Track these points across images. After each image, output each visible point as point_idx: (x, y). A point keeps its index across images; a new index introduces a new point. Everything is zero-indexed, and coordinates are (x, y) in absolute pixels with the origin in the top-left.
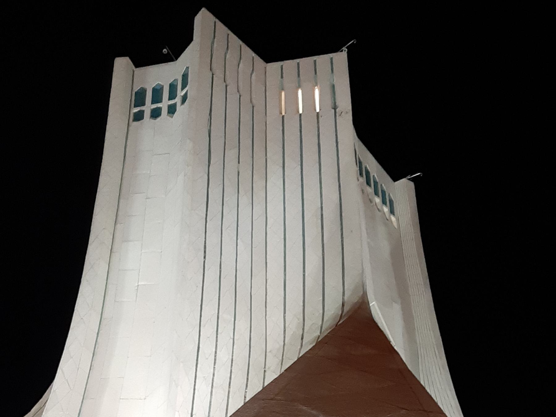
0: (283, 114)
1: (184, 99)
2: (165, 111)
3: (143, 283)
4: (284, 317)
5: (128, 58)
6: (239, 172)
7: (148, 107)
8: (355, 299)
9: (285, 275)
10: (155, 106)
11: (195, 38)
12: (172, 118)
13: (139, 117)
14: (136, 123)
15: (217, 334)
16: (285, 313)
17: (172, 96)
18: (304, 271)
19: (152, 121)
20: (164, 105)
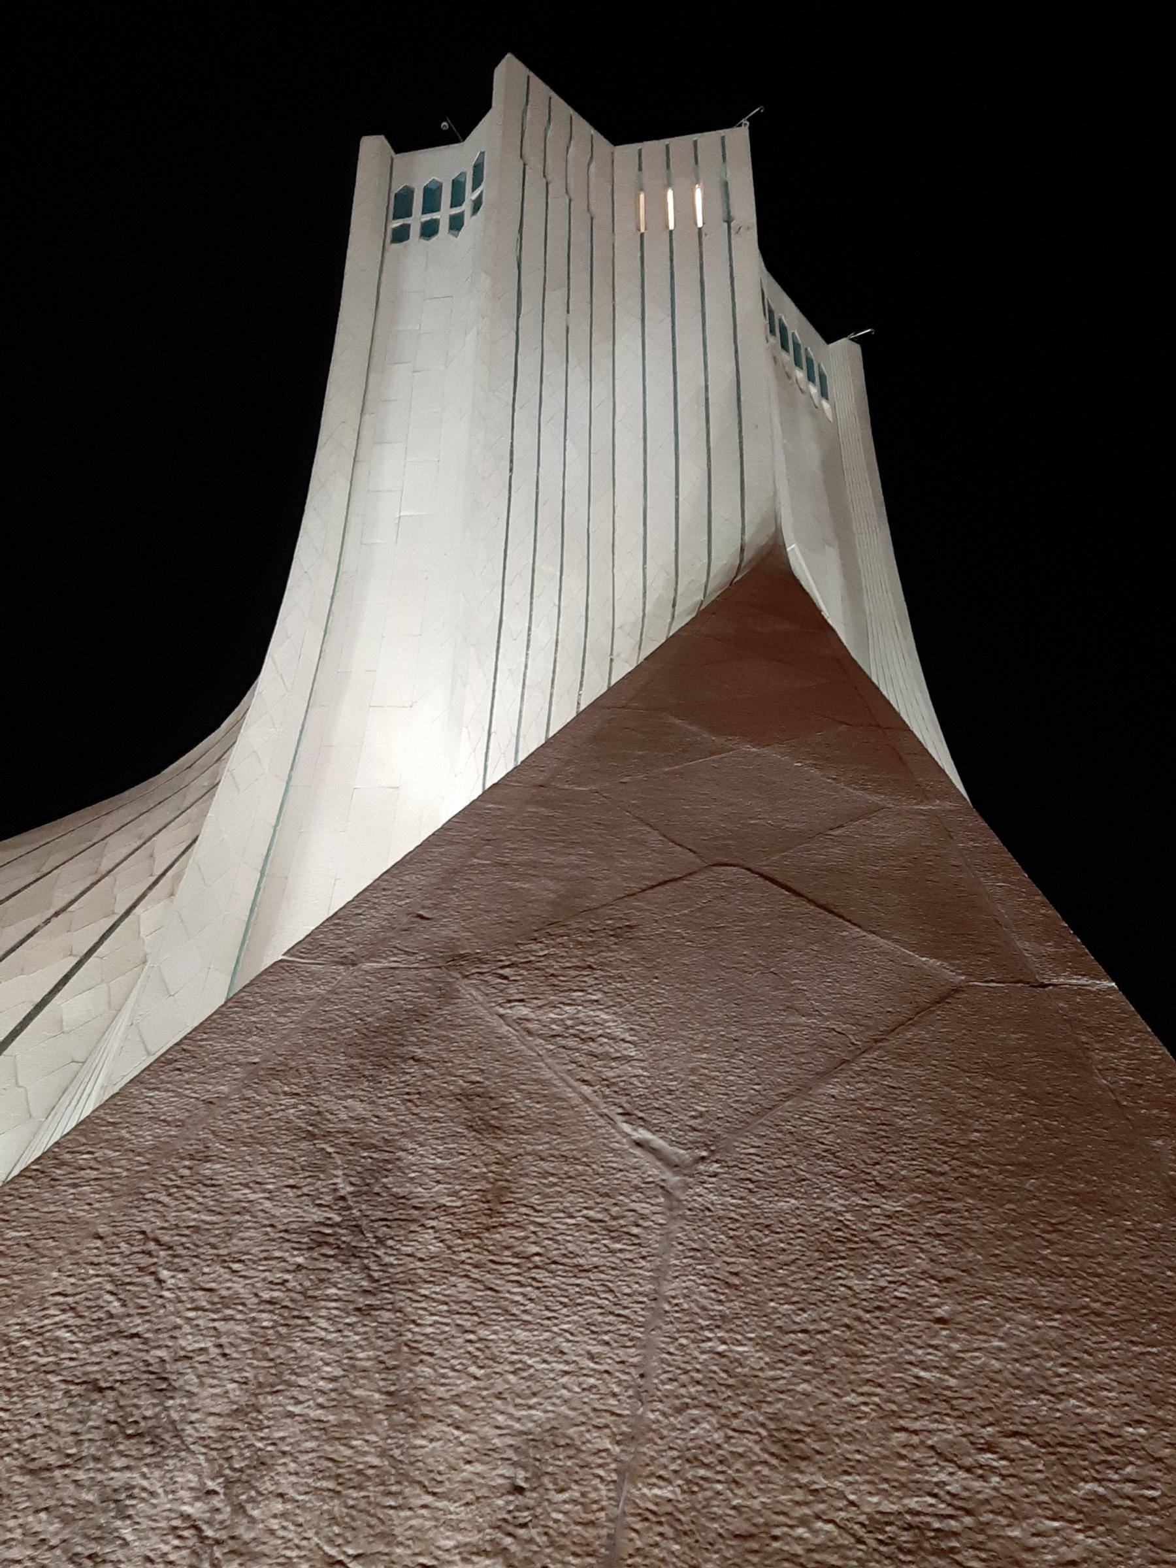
0: (643, 230)
1: (477, 205)
2: (444, 226)
3: (408, 513)
4: (644, 569)
5: (382, 137)
6: (568, 328)
7: (417, 219)
8: (762, 540)
9: (645, 499)
10: (427, 217)
11: (494, 104)
13: (401, 235)
14: (396, 246)
15: (532, 598)
16: (645, 563)
17: (457, 201)
18: (677, 493)
19: (424, 242)
20: (443, 216)
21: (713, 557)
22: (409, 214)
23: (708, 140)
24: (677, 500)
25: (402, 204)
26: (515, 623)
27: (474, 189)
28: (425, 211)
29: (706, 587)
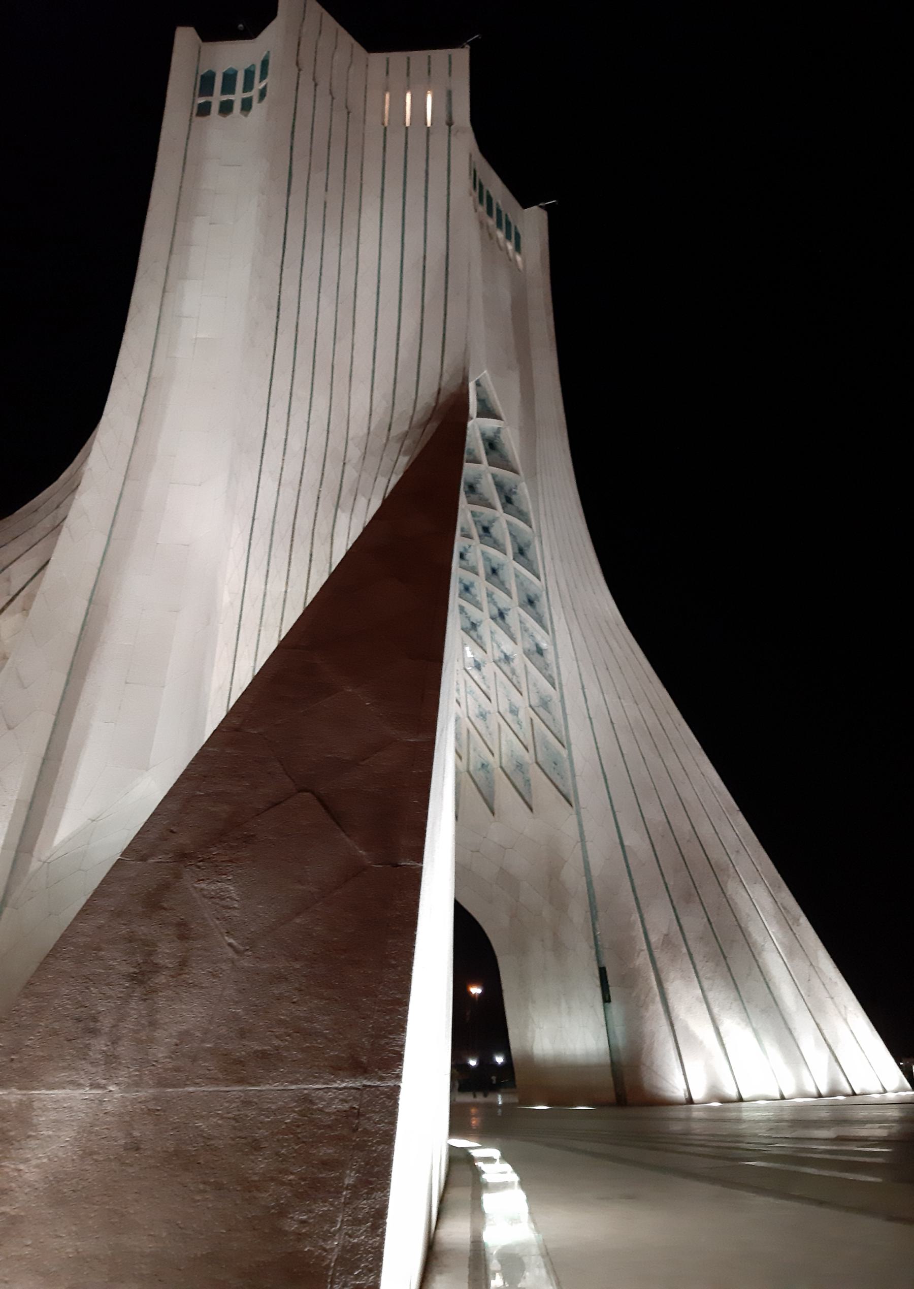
0: (386, 124)
1: (263, 94)
2: (237, 106)
7: (217, 98)
11: (279, 13)
12: (246, 116)
13: (204, 110)
14: (200, 119)
17: (248, 86)
19: (220, 117)
20: (237, 97)
21: (419, 394)
22: (211, 94)
23: (439, 56)
24: (398, 344)
25: (206, 83)
26: (276, 433)
27: (261, 81)
28: (224, 91)
29: (412, 419)
